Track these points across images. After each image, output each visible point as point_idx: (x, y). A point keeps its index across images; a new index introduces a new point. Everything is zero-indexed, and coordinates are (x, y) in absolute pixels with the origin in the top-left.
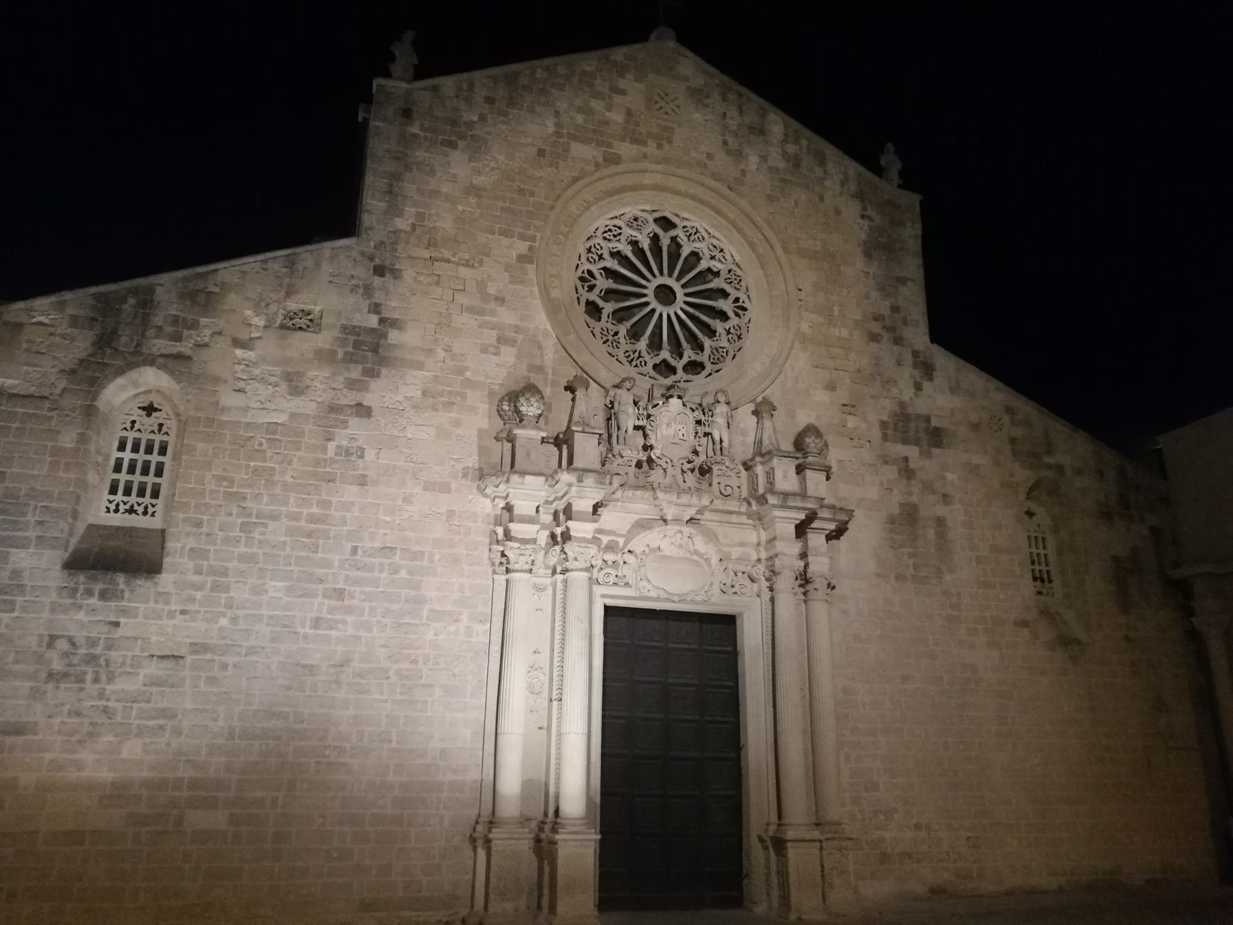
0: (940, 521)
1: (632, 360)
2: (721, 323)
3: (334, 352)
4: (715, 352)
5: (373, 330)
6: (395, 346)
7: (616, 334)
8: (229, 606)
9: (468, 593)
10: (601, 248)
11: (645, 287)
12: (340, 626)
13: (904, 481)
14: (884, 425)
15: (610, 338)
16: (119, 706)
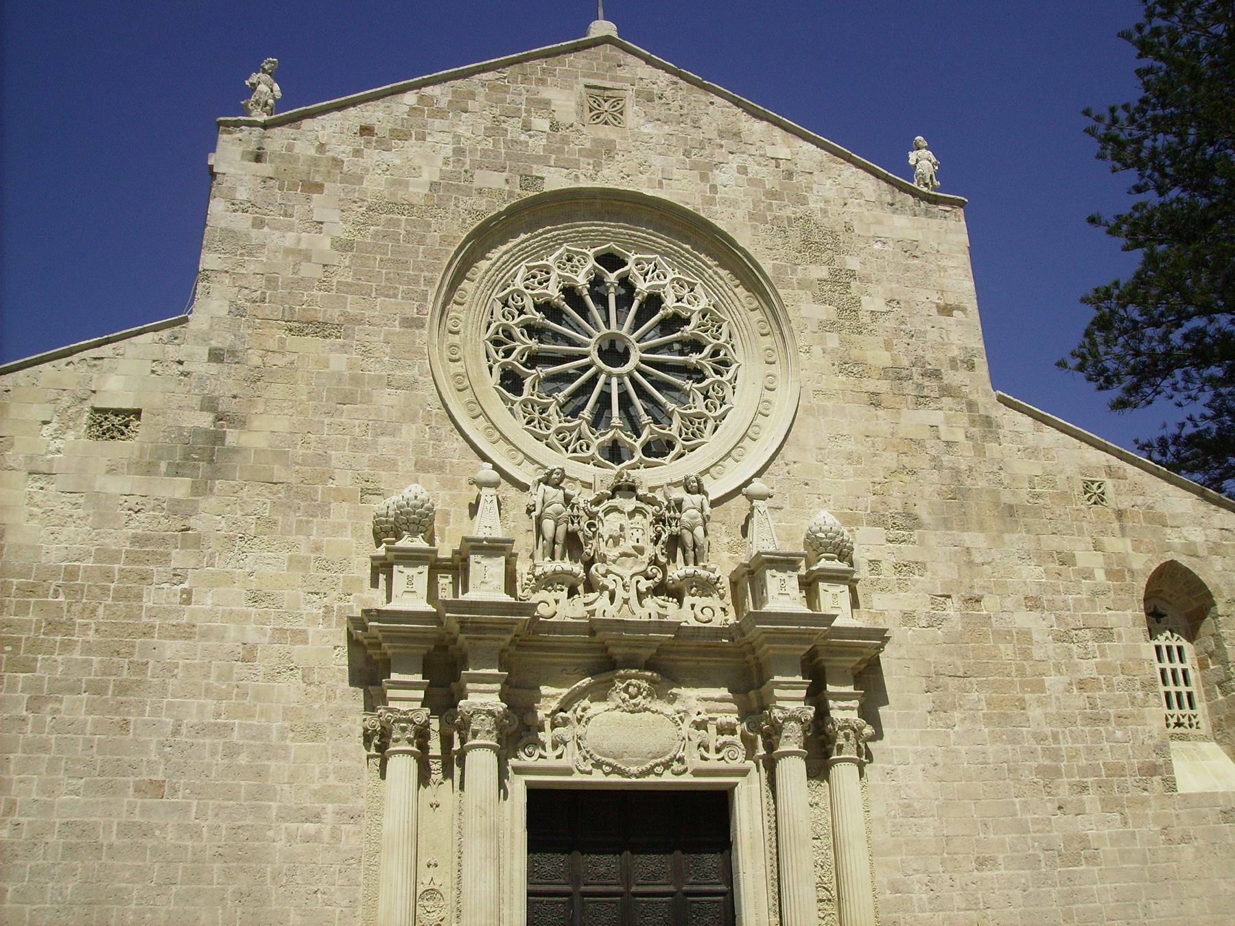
1: (568, 444)
2: (695, 385)
5: (206, 432)
6: (235, 450)
9: (332, 780)
10: (522, 300)
11: (587, 345)
12: (157, 832)
15: (537, 415)
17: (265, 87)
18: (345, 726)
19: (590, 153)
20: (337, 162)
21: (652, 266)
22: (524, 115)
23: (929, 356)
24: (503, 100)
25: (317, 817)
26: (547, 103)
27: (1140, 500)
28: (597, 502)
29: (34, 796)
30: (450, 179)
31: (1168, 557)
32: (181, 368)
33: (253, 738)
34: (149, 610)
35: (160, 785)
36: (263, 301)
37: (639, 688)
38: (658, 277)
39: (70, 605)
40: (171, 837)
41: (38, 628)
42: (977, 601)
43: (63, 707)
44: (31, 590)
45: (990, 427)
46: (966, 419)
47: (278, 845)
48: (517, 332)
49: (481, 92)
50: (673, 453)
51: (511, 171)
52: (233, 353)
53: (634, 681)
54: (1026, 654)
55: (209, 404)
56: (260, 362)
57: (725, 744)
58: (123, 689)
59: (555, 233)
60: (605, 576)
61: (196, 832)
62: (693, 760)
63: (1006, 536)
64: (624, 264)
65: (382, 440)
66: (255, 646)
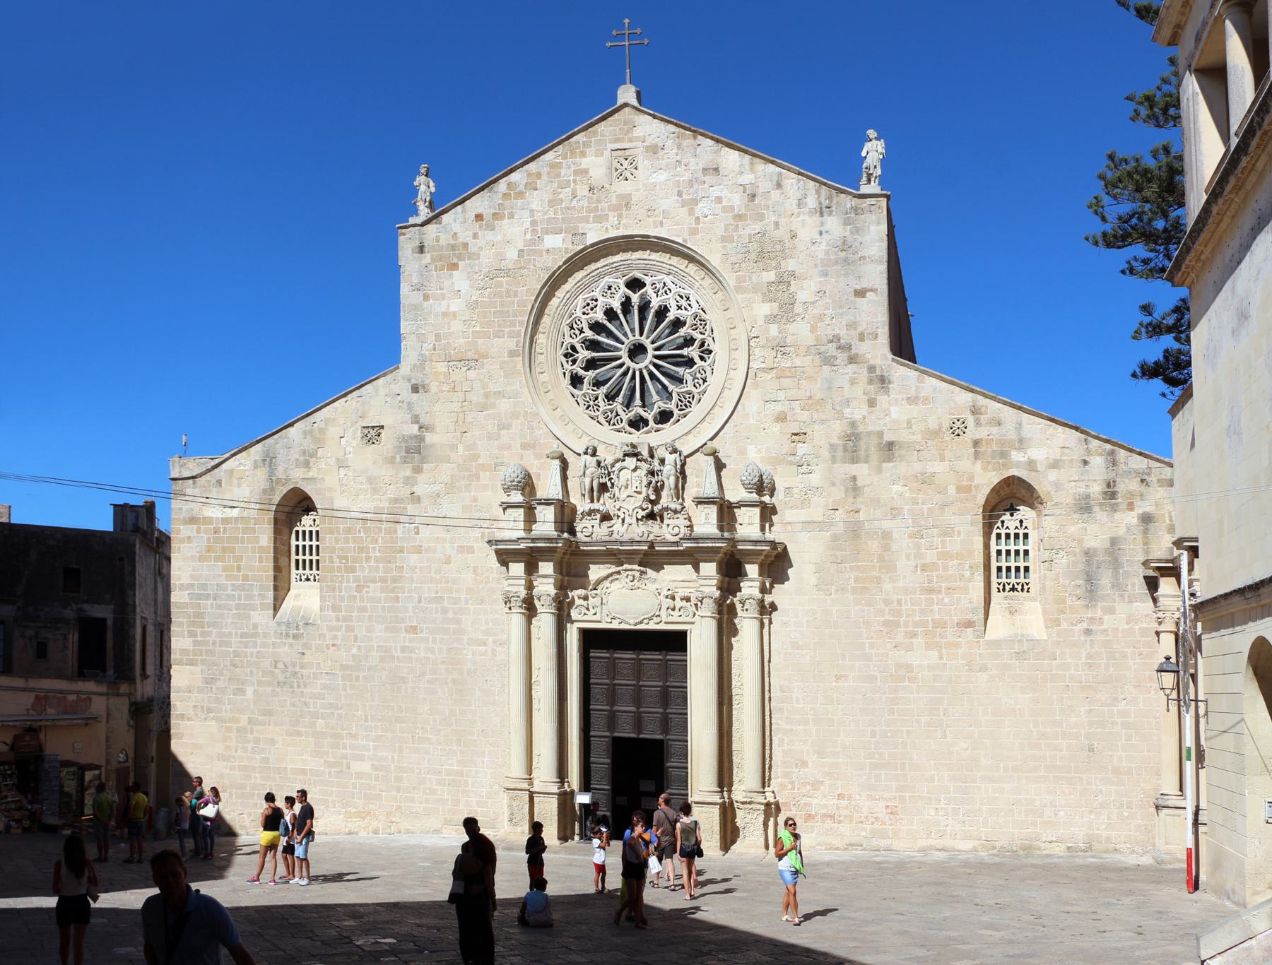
0: (886, 535)
2: (688, 371)
3: (393, 457)
4: (683, 400)
5: (416, 436)
6: (431, 446)
7: (597, 398)
8: (356, 640)
13: (851, 500)
14: (833, 447)
15: (591, 403)
16: (311, 701)
17: (425, 186)
18: (494, 597)
19: (616, 208)
20: (465, 245)
21: (662, 285)
22: (573, 184)
23: (843, 332)
24: (559, 175)
25: (485, 644)
26: (586, 171)
27: (995, 430)
28: (617, 461)
29: (365, 634)
30: (529, 246)
31: (1010, 473)
32: (399, 398)
33: (454, 604)
34: (401, 538)
35: (415, 628)
36: (435, 349)
37: (634, 577)
38: (666, 292)
39: (366, 537)
40: (423, 654)
41: (355, 550)
42: (857, 512)
43: (370, 590)
44: (348, 531)
45: (883, 384)
46: (865, 380)
47: (468, 657)
48: (578, 347)
49: (546, 169)
50: (672, 420)
51: (565, 232)
52: (423, 387)
53: (630, 573)
54: (886, 548)
55: (416, 419)
56: (437, 391)
57: (682, 608)
58: (395, 580)
59: (598, 271)
60: (619, 510)
61: (433, 652)
62: (664, 618)
63: (885, 465)
64: (643, 285)
65: (502, 432)
66: (450, 556)
